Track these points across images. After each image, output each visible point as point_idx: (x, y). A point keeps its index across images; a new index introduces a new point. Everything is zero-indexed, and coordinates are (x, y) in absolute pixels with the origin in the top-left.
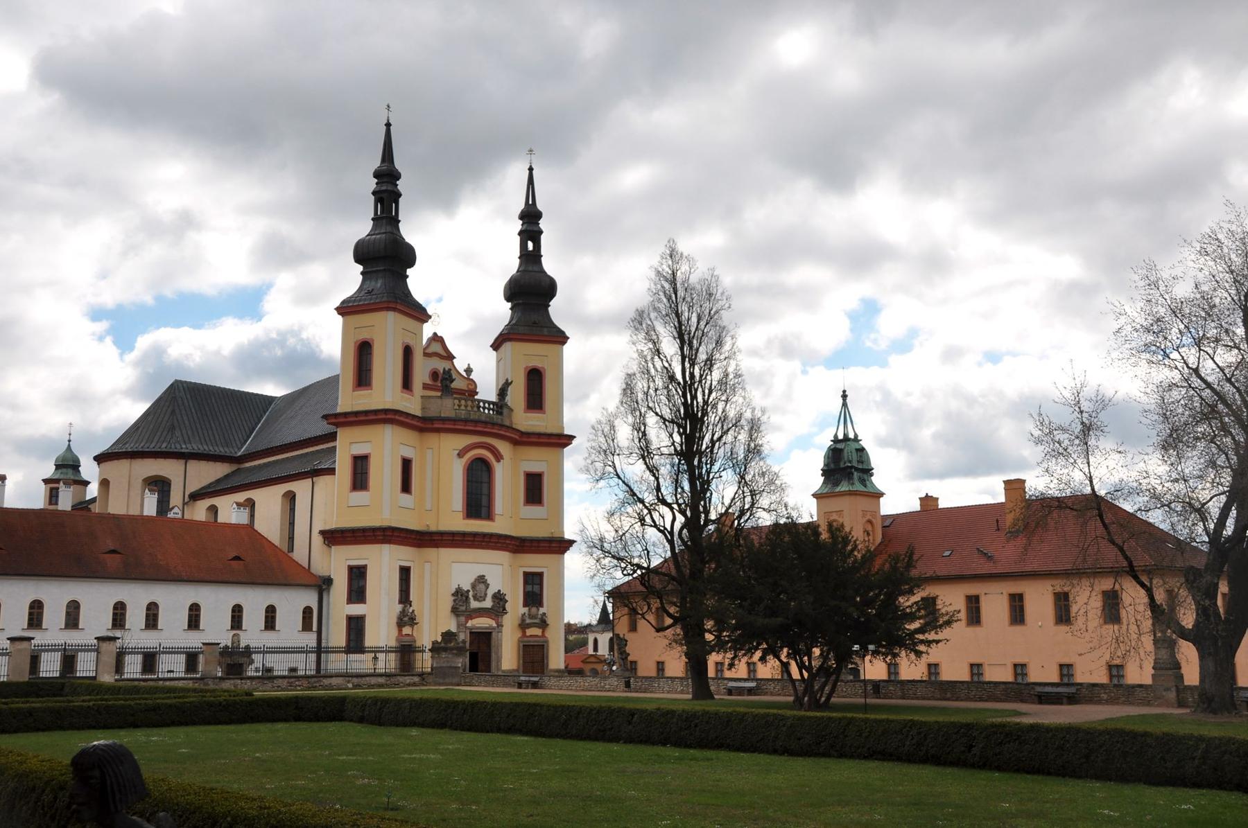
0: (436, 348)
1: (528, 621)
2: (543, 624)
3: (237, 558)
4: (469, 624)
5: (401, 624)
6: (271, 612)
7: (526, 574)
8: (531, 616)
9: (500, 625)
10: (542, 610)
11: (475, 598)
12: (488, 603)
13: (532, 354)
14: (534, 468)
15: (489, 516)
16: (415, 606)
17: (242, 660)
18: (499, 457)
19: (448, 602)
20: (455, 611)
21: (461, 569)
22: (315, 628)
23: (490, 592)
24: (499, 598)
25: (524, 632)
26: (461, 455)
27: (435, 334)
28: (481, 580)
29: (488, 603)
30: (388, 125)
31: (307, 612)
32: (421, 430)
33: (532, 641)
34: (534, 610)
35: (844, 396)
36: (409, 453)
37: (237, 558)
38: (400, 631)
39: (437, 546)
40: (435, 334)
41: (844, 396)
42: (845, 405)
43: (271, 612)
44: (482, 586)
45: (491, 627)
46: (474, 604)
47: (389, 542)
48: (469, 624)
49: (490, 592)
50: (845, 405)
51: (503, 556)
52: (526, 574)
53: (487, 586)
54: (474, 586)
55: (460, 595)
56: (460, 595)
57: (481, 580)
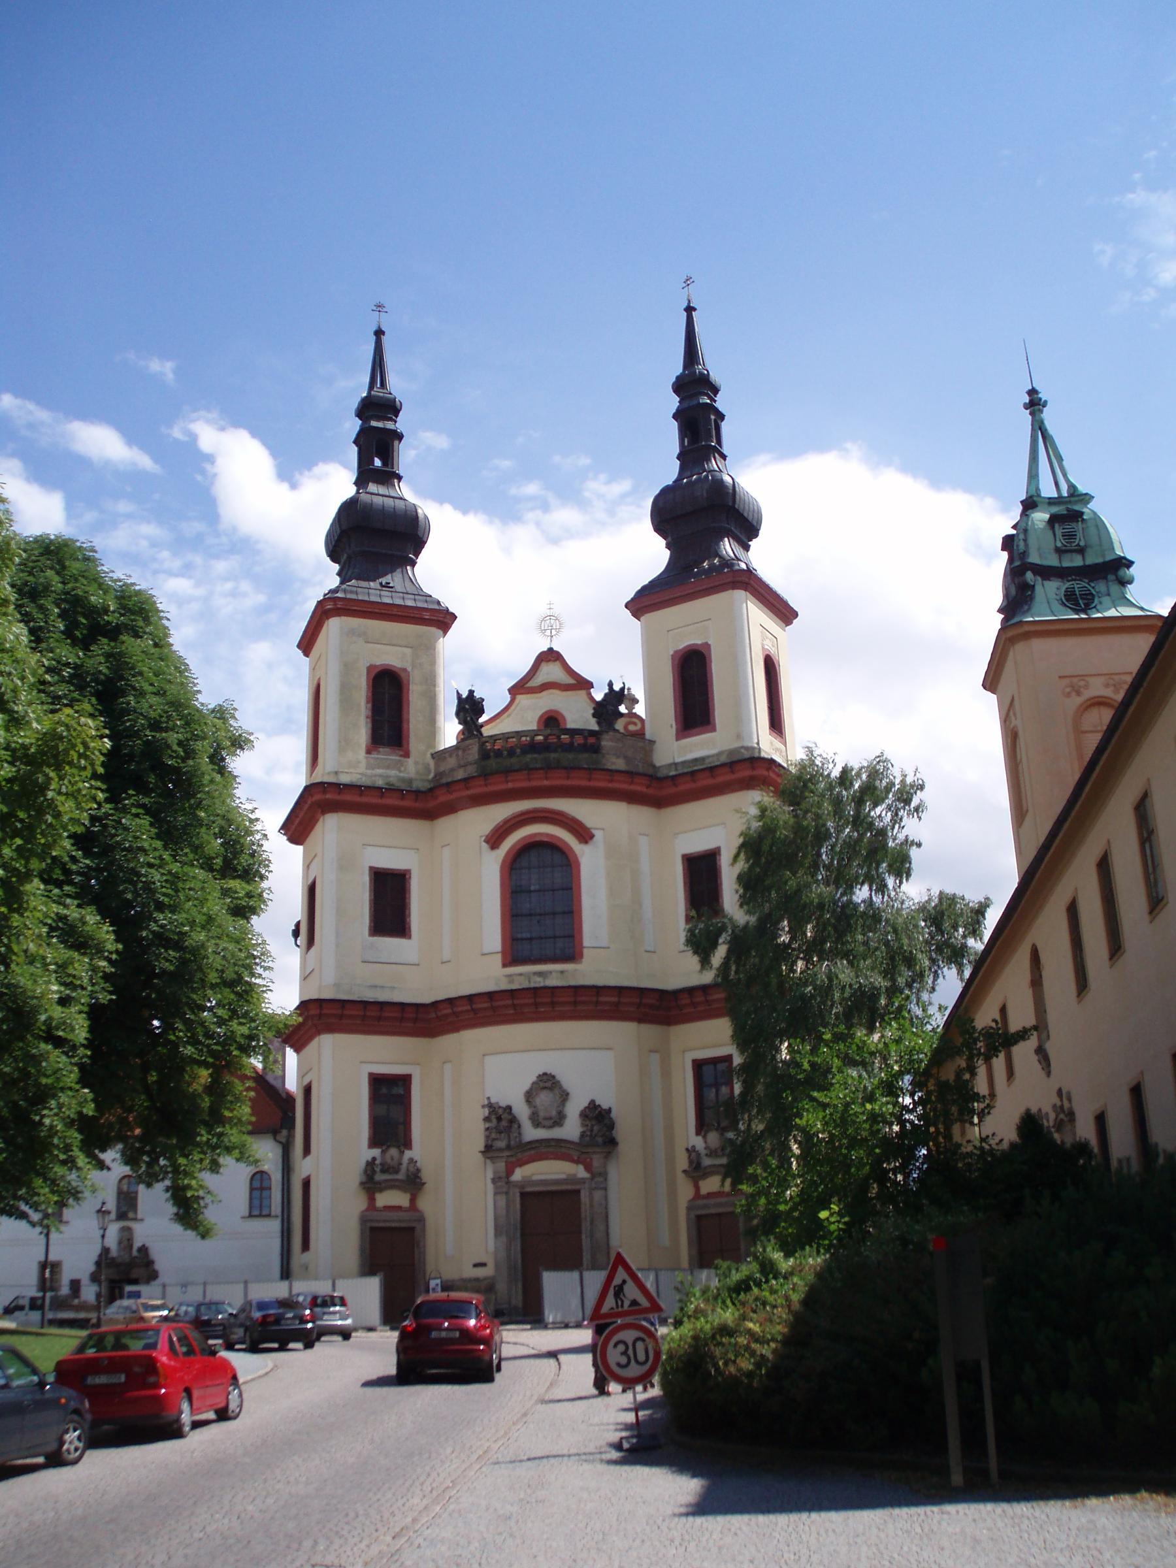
0: (550, 672)
1: (707, 1162)
4: (518, 1175)
8: (712, 1153)
9: (599, 1178)
11: (536, 1122)
13: (688, 622)
15: (572, 953)
16: (421, 1150)
18: (584, 834)
19: (475, 1133)
20: (489, 1150)
21: (501, 1065)
23: (573, 1110)
24: (597, 1116)
25: (697, 1188)
26: (494, 839)
27: (551, 650)
28: (547, 1082)
29: (572, 1129)
32: (430, 815)
35: (1035, 403)
38: (372, 1199)
39: (456, 1028)
40: (551, 650)
41: (1035, 403)
42: (1039, 428)
44: (544, 1099)
45: (572, 1180)
46: (531, 1133)
47: (331, 1029)
49: (573, 1110)
50: (1039, 428)
51: (621, 1034)
53: (565, 1096)
54: (529, 1096)
55: (500, 1119)
56: (500, 1119)
57: (547, 1082)
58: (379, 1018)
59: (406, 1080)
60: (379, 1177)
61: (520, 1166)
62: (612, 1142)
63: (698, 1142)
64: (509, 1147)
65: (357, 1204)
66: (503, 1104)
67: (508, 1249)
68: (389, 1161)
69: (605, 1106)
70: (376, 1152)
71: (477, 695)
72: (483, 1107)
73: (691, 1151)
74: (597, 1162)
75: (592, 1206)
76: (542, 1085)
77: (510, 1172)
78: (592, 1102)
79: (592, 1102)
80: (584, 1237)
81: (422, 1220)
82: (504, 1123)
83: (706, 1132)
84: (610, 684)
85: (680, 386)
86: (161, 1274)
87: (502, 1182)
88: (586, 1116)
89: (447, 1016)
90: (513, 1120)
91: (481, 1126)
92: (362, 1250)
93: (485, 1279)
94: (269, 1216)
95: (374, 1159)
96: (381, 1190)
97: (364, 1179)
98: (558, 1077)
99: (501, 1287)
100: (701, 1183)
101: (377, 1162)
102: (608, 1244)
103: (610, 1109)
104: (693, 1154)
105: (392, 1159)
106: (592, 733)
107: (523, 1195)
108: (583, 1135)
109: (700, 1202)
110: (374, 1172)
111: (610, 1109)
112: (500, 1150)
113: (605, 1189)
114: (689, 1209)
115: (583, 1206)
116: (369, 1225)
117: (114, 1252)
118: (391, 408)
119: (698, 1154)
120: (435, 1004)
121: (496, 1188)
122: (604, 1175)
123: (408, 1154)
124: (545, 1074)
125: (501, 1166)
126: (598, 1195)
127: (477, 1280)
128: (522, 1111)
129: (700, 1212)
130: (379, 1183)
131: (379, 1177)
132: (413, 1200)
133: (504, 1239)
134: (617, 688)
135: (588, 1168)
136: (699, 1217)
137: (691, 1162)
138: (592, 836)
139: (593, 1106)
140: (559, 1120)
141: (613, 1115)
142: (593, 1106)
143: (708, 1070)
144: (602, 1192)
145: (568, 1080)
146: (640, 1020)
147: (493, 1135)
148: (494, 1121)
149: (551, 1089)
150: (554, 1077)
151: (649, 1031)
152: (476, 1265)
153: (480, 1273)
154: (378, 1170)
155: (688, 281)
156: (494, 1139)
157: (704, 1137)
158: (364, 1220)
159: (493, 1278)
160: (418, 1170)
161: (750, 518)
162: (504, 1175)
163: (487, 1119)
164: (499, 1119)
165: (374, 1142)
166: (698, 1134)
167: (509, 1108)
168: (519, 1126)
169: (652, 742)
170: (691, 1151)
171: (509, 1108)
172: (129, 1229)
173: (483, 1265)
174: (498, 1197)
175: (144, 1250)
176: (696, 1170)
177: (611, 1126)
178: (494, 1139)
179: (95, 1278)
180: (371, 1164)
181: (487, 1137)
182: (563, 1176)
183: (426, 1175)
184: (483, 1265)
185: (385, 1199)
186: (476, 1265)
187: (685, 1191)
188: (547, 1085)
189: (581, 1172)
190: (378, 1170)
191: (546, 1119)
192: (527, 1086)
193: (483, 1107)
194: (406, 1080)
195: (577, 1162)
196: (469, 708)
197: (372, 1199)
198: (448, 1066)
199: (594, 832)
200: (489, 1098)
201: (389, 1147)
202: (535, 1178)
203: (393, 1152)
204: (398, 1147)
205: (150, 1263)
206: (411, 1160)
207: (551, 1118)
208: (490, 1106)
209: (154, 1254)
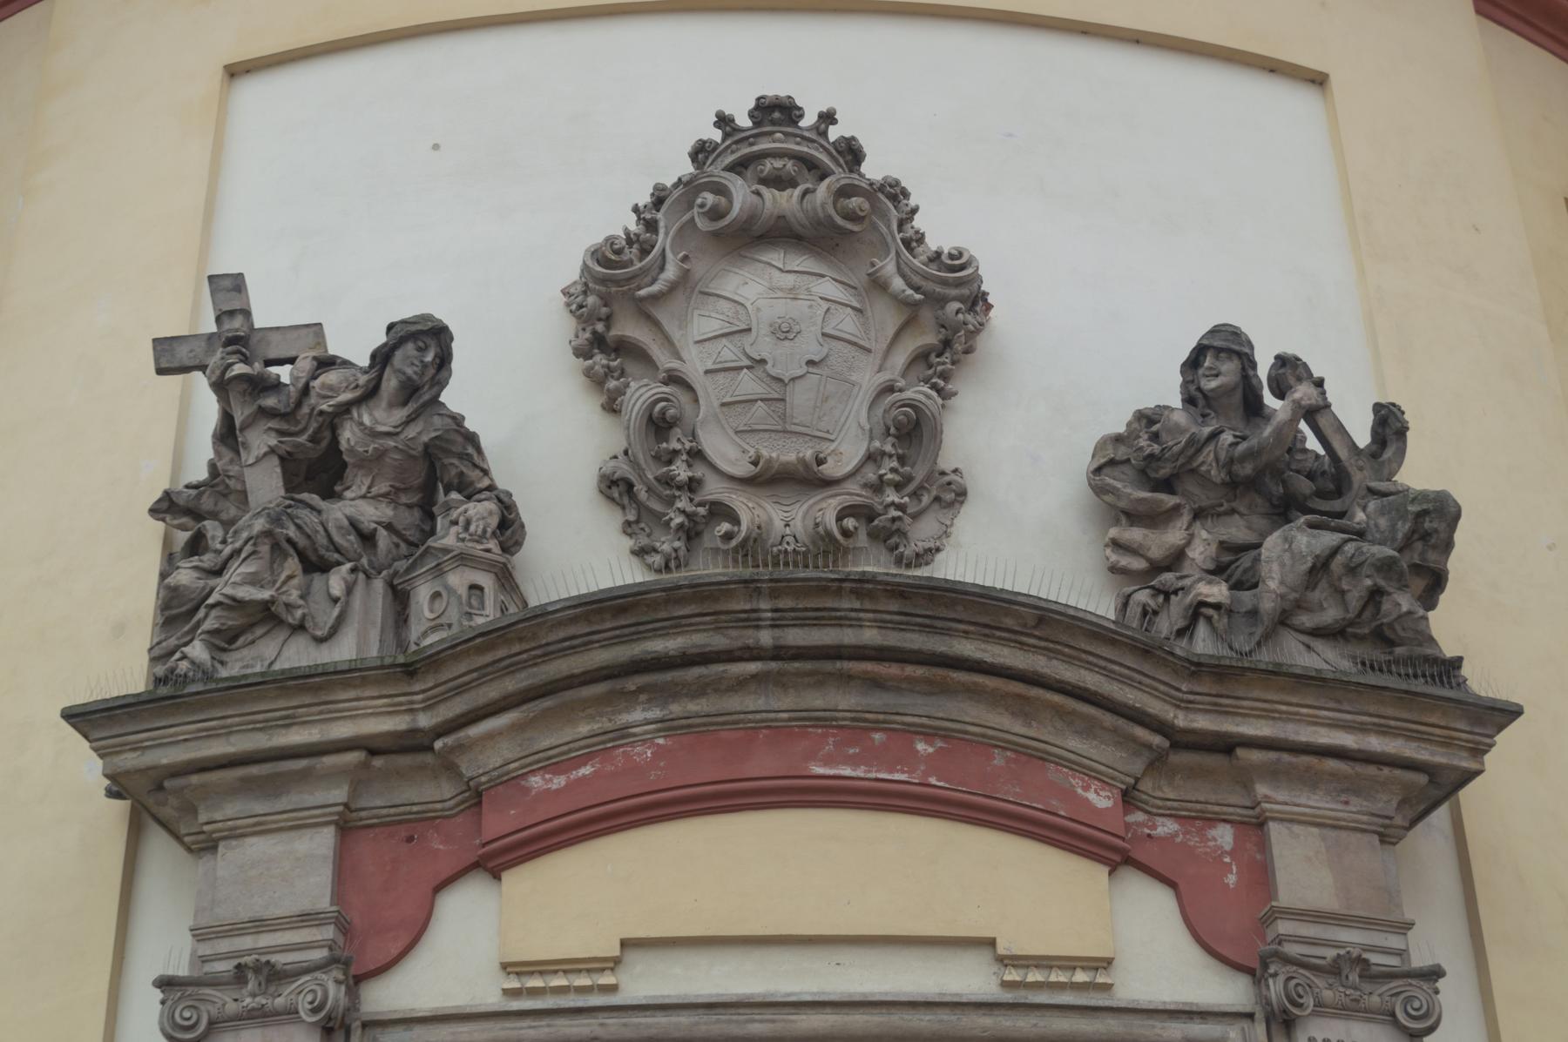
53: (945, 312)
54: (615, 311)
61: (493, 863)
72: (170, 358)
74: (1305, 870)
78: (1222, 347)
82: (360, 505)
103: (1390, 425)
125: (288, 871)
128: (532, 418)
135: (1236, 929)
147: (237, 584)
149: (819, 239)
164: (317, 470)
168: (509, 528)
181: (176, 611)
182: (970, 979)
188: (784, 202)
193: (170, 358)
195: (1117, 856)
200: (228, 288)
202: (644, 982)
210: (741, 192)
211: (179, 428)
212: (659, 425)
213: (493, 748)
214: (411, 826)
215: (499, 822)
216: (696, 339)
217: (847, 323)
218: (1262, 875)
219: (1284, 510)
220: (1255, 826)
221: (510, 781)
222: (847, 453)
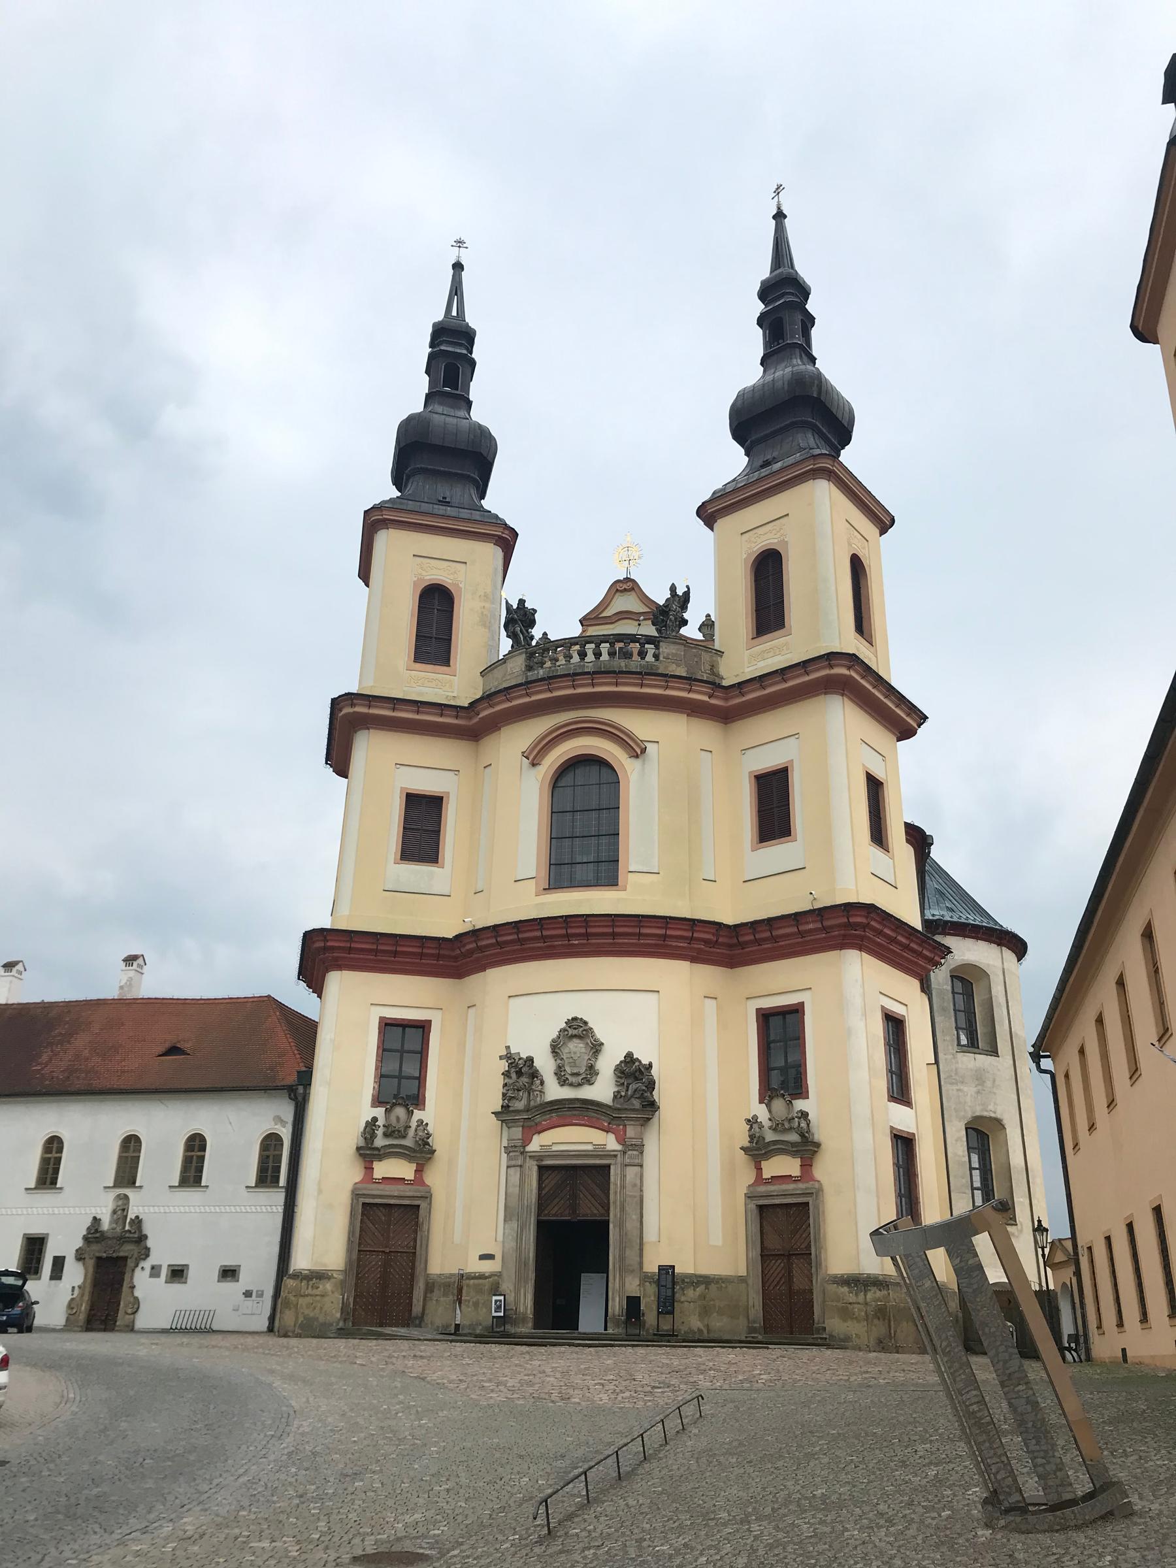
1: (770, 1136)
2: (807, 1148)
3: (173, 1050)
4: (536, 1144)
5: (368, 1153)
6: (196, 1145)
7: (766, 1017)
10: (800, 1105)
11: (563, 1082)
12: (603, 1090)
14: (767, 760)
16: (434, 1113)
17: (127, 1250)
18: (636, 750)
20: (505, 1114)
21: (524, 1009)
22: (283, 1181)
23: (607, 1064)
24: (634, 1073)
25: (759, 1169)
26: (534, 757)
28: (577, 1029)
29: (603, 1090)
30: (458, 267)
31: (271, 1143)
33: (780, 1194)
34: (779, 1105)
36: (426, 784)
37: (173, 1050)
39: (483, 968)
40: (628, 580)
43: (196, 1145)
44: (576, 1047)
46: (554, 1091)
47: (340, 968)
48: (536, 1144)
49: (607, 1064)
52: (766, 1017)
53: (596, 1048)
55: (520, 1072)
56: (520, 1072)
57: (577, 1029)
58: (396, 954)
59: (423, 1027)
60: (380, 1142)
61: (539, 1133)
62: (651, 1106)
63: (762, 1113)
64: (527, 1110)
65: (352, 1174)
66: (524, 1055)
67: (519, 1238)
68: (393, 1121)
69: (645, 1062)
70: (380, 1112)
71: (528, 605)
72: (501, 1058)
73: (752, 1122)
74: (631, 1131)
75: (623, 1187)
76: (571, 1032)
77: (527, 1141)
78: (629, 1055)
79: (629, 1055)
80: (611, 1226)
81: (428, 1197)
82: (524, 1080)
83: (771, 1098)
84: (673, 589)
85: (766, 292)
86: (152, 1253)
87: (516, 1151)
88: (623, 1072)
89: (471, 952)
90: (534, 1074)
91: (501, 1081)
92: (351, 1233)
93: (492, 1275)
94: (278, 1187)
95: (375, 1119)
96: (380, 1158)
97: (362, 1143)
98: (590, 1025)
99: (507, 1286)
100: (764, 1165)
101: (380, 1123)
102: (641, 1238)
103: (650, 1065)
104: (755, 1126)
105: (398, 1119)
106: (650, 640)
107: (542, 1169)
108: (616, 1096)
109: (762, 1189)
110: (373, 1136)
111: (650, 1065)
112: (518, 1112)
113: (641, 1166)
114: (749, 1197)
115: (612, 1186)
116: (362, 1200)
117: (106, 1225)
118: (467, 337)
119: (761, 1126)
120: (457, 937)
121: (510, 1159)
122: (640, 1148)
123: (418, 1115)
124: (575, 1019)
125: (517, 1132)
126: (631, 1172)
127: (482, 1276)
128: (545, 1064)
129: (761, 1202)
130: (377, 1149)
131: (380, 1142)
132: (419, 1171)
133: (514, 1224)
134: (680, 592)
135: (621, 1140)
136: (761, 1208)
137: (752, 1137)
138: (644, 750)
139: (629, 1059)
140: (589, 1077)
141: (654, 1072)
142: (629, 1059)
143: (775, 1022)
144: (637, 1169)
145: (600, 1032)
146: (694, 960)
147: (510, 1094)
148: (514, 1076)
150: (586, 1023)
151: (706, 976)
152: (483, 1257)
153: (487, 1267)
154: (380, 1132)
155: (778, 190)
156: (511, 1098)
157: (768, 1106)
158: (356, 1194)
159: (499, 1275)
160: (429, 1135)
161: (839, 416)
162: (519, 1143)
163: (506, 1074)
164: (519, 1073)
165: (377, 1101)
166: (761, 1102)
167: (530, 1060)
168: (542, 1083)
169: (720, 653)
170: (752, 1122)
171: (530, 1060)
172: (126, 1197)
173: (490, 1257)
174: (512, 1171)
175: (137, 1222)
176: (758, 1150)
177: (651, 1085)
178: (511, 1098)
179: (80, 1256)
180: (372, 1124)
181: (504, 1095)
182: (590, 1147)
183: (437, 1142)
184: (490, 1257)
185: (383, 1169)
186: (483, 1257)
187: (747, 1177)
188: (575, 1032)
189: (611, 1143)
190: (380, 1132)
191: (573, 1074)
192: (555, 1034)
193: (501, 1058)
194: (423, 1027)
196: (520, 619)
197: (369, 1169)
198: (471, 1011)
199: (648, 745)
200: (508, 1048)
201: (394, 1105)
202: (555, 1148)
203: (400, 1111)
204: (406, 1106)
205: (142, 1238)
206: (420, 1122)
207: (577, 1074)
208: (509, 1057)
209: (147, 1229)
210: (571, 1032)
211: (504, 1065)
212: (559, 1067)
213: (538, 1119)
214: (530, 1127)
215: (539, 1128)
216: (565, 1052)
217: (583, 1050)
218: (625, 1132)
219: (636, 1079)
220: (625, 1126)
221: (540, 1123)
222: (582, 1071)
